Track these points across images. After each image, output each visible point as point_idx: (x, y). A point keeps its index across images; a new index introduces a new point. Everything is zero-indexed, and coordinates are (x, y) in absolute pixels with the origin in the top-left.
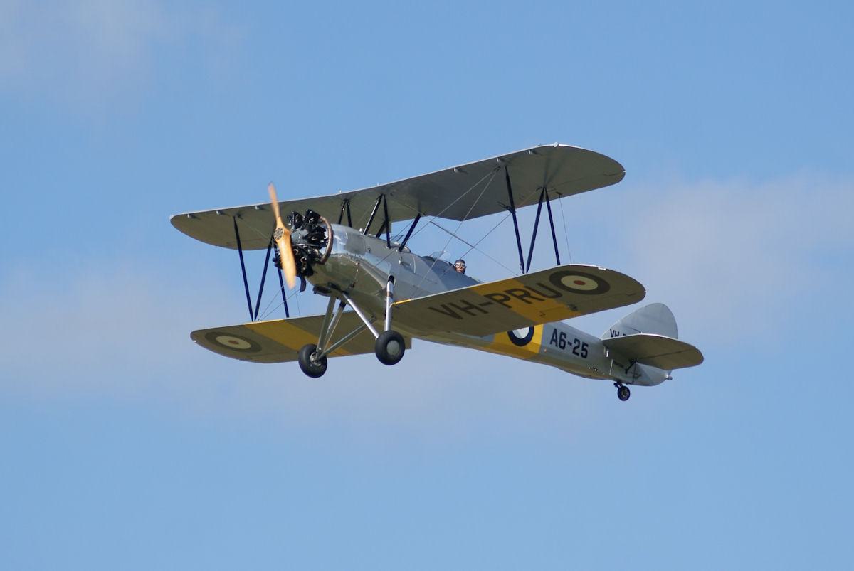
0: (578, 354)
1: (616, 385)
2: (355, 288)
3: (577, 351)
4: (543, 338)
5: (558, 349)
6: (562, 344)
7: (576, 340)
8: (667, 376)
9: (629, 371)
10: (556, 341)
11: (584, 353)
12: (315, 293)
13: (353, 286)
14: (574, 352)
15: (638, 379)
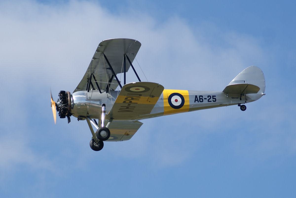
0: (211, 101)
1: (239, 105)
2: (89, 114)
3: (210, 100)
4: (190, 101)
5: (200, 103)
6: (201, 100)
7: (208, 96)
8: (263, 94)
9: (241, 98)
10: (197, 100)
11: (214, 100)
12: (78, 121)
13: (88, 114)
14: (209, 101)
15: (247, 100)
